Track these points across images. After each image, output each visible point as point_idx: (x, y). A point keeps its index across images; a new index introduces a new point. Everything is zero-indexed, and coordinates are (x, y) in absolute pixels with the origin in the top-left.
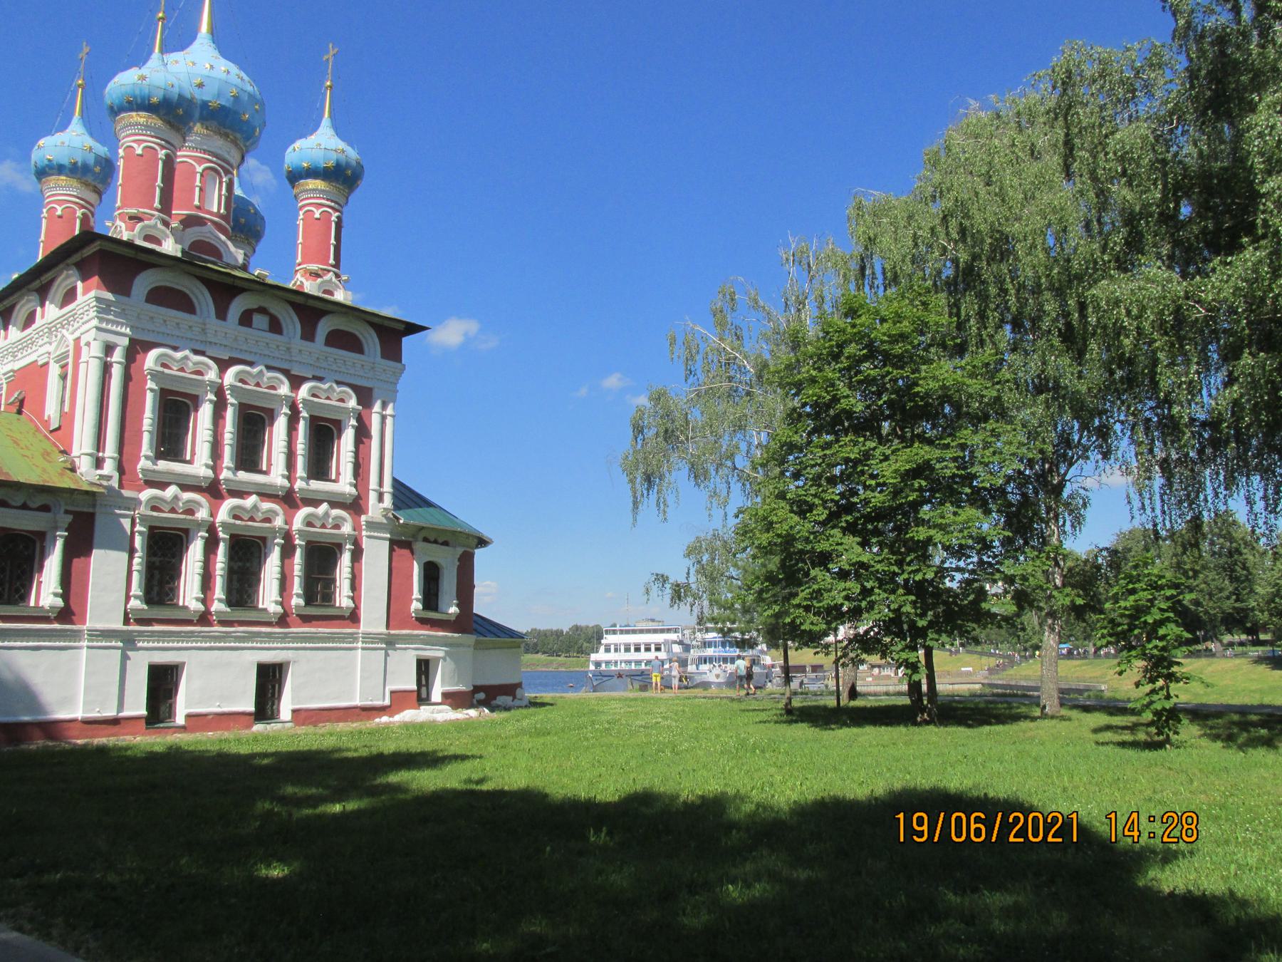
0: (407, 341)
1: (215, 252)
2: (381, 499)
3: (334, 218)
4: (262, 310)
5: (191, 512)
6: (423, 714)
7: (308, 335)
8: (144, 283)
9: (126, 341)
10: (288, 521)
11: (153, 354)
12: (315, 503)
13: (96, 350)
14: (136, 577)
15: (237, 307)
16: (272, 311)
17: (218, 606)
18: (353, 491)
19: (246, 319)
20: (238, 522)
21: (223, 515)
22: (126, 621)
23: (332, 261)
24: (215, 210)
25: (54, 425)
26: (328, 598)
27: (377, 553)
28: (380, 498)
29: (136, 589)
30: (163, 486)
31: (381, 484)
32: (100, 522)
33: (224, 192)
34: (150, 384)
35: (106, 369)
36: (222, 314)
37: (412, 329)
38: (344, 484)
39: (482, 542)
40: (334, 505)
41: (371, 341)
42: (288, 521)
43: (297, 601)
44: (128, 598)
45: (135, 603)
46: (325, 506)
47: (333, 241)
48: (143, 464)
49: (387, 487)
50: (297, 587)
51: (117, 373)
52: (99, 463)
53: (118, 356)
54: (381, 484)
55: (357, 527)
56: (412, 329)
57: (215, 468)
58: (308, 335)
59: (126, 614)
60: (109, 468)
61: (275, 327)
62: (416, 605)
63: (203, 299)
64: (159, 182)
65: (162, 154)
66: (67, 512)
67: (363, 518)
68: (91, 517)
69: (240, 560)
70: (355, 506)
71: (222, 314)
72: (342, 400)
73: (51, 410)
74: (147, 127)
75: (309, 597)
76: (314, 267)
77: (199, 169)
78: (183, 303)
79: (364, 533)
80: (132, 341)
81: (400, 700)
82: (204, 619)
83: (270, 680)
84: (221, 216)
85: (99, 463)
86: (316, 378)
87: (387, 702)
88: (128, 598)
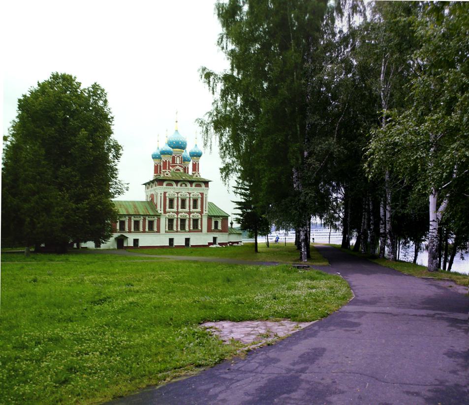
1: (179, 170)
4: (184, 183)
6: (214, 246)
7: (191, 186)
8: (165, 184)
10: (189, 216)
13: (159, 195)
15: (179, 184)
17: (179, 230)
19: (181, 186)
21: (179, 216)
27: (205, 220)
29: (167, 227)
32: (161, 219)
34: (167, 198)
36: (177, 186)
37: (211, 181)
38: (199, 210)
41: (203, 185)
42: (189, 216)
43: (192, 228)
45: (167, 230)
48: (167, 210)
49: (207, 209)
50: (191, 226)
51: (162, 198)
52: (161, 210)
53: (163, 195)
55: (202, 216)
56: (211, 181)
57: (178, 209)
58: (191, 186)
60: (162, 212)
61: (186, 186)
62: (213, 228)
63: (174, 184)
67: (203, 214)
68: (160, 218)
70: (201, 213)
71: (177, 186)
73: (155, 202)
75: (194, 228)
78: (172, 185)
81: (210, 244)
82: (177, 232)
83: (187, 240)
87: (207, 244)
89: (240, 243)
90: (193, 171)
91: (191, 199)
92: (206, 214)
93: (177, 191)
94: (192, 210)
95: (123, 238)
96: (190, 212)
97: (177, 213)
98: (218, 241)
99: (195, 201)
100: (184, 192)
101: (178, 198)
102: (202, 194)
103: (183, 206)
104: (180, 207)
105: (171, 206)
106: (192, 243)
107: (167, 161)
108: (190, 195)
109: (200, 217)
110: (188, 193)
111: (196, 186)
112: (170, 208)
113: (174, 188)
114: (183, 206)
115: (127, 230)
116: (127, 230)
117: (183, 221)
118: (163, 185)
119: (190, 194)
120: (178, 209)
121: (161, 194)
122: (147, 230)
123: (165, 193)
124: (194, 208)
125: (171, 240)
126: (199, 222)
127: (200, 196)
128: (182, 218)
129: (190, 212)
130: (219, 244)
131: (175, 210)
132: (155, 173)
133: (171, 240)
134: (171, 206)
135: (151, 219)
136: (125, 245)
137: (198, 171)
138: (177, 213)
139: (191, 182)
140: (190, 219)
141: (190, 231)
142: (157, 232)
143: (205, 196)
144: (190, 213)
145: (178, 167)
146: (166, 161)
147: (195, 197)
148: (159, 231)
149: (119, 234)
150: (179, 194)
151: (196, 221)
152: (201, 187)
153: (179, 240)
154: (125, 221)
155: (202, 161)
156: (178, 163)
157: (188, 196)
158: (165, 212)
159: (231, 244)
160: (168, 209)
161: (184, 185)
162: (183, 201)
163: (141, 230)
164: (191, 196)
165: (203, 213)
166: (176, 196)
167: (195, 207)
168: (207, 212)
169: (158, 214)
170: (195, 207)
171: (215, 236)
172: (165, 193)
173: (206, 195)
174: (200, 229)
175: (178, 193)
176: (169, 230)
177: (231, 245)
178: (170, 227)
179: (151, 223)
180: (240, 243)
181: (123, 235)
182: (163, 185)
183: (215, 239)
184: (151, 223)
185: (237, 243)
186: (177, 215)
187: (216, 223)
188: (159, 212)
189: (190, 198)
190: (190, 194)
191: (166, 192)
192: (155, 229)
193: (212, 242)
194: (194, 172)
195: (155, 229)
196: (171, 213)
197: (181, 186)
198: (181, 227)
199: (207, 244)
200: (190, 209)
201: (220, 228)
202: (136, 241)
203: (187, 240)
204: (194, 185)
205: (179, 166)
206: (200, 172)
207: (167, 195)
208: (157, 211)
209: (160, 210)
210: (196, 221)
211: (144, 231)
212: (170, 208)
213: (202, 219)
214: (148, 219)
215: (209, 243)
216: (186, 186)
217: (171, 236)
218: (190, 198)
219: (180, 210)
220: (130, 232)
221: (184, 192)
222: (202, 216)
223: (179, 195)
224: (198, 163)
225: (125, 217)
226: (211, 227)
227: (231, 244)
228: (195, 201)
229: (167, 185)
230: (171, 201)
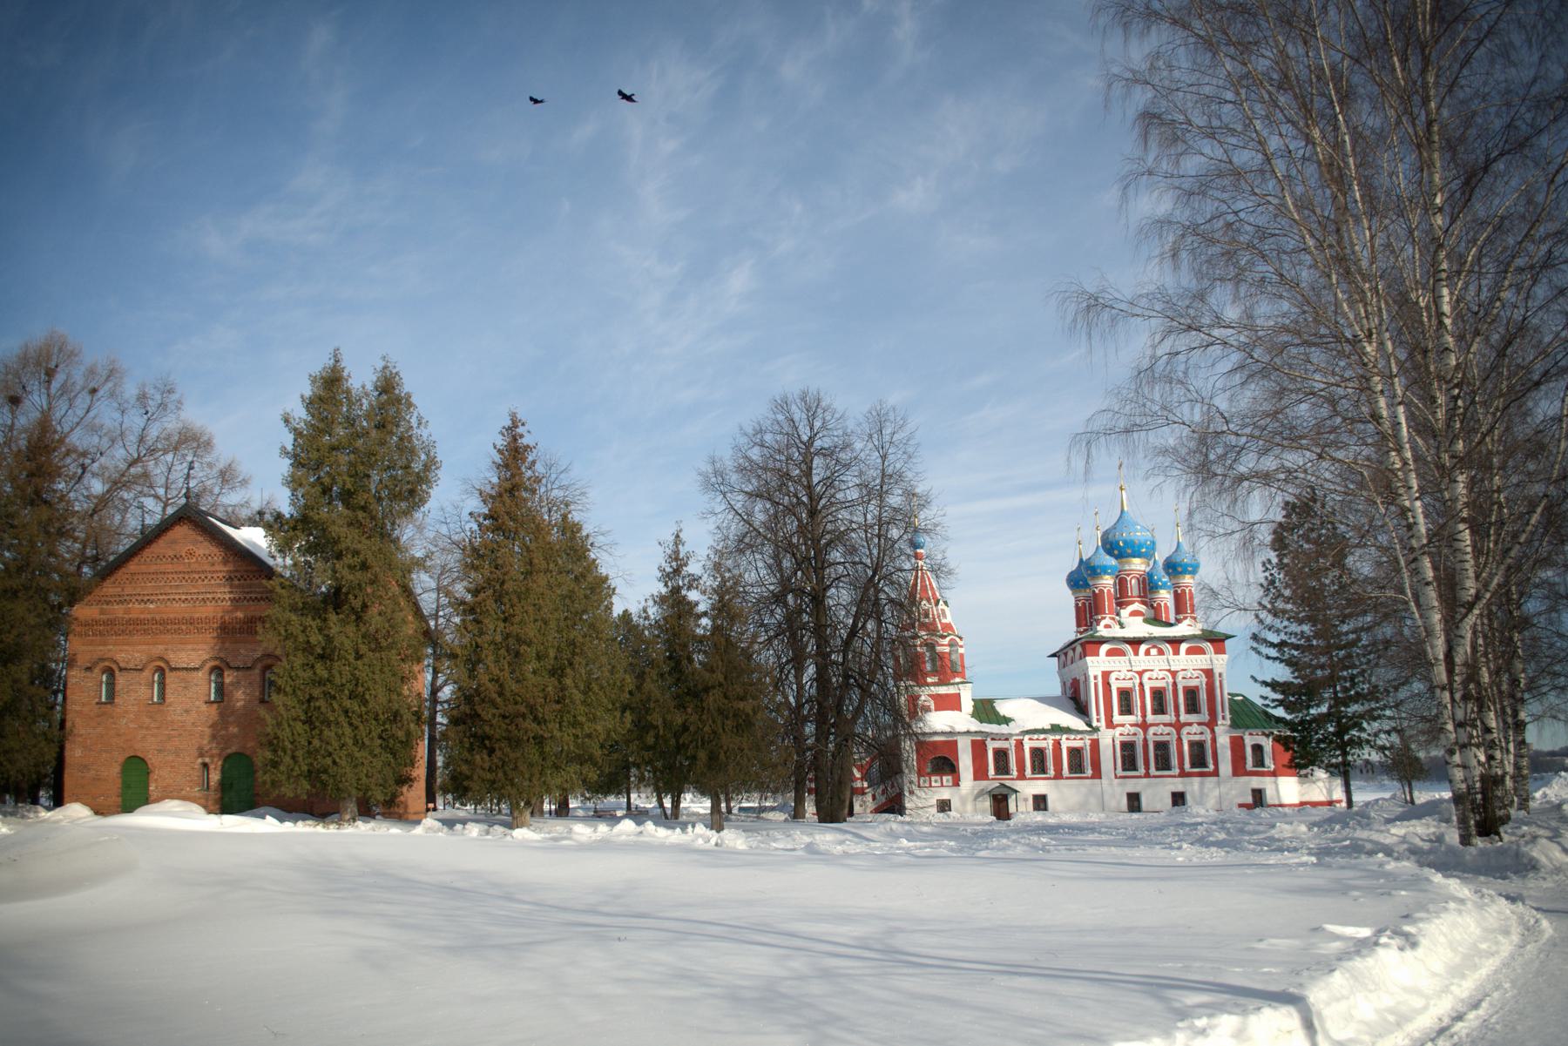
0: (1227, 642)
7: (1176, 652)
10: (1179, 733)
12: (1190, 724)
15: (1143, 648)
17: (1153, 771)
19: (1147, 653)
26: (1204, 765)
36: (1136, 653)
38: (1205, 716)
42: (1179, 733)
45: (1120, 772)
57: (1144, 715)
58: (1176, 652)
60: (1103, 724)
61: (1161, 652)
70: (1211, 724)
71: (1136, 653)
75: (1193, 765)
78: (1122, 653)
82: (1147, 775)
90: (1178, 612)
94: (1184, 718)
95: (1005, 791)
103: (1160, 709)
112: (1122, 713)
115: (1015, 773)
118: (1097, 654)
119: (1174, 674)
120: (1144, 715)
123: (1106, 675)
124: (1188, 712)
127: (1204, 680)
132: (1078, 625)
134: (1127, 709)
140: (1180, 740)
141: (1183, 774)
142: (1093, 777)
148: (1097, 774)
150: (1146, 675)
156: (1136, 592)
158: (1110, 724)
160: (1117, 718)
161: (1154, 651)
162: (1158, 695)
163: (1052, 773)
164: (1180, 675)
166: (1137, 681)
170: (1193, 707)
172: (1106, 675)
174: (1211, 767)
175: (1141, 674)
176: (1124, 770)
178: (1129, 762)
182: (1097, 654)
186: (1145, 732)
187: (1258, 749)
188: (1095, 724)
195: (1089, 772)
197: (1147, 653)
204: (1184, 647)
207: (1112, 680)
211: (1058, 776)
213: (1214, 740)
220: (1022, 776)
222: (1213, 731)
223: (1145, 680)
229: (1110, 653)
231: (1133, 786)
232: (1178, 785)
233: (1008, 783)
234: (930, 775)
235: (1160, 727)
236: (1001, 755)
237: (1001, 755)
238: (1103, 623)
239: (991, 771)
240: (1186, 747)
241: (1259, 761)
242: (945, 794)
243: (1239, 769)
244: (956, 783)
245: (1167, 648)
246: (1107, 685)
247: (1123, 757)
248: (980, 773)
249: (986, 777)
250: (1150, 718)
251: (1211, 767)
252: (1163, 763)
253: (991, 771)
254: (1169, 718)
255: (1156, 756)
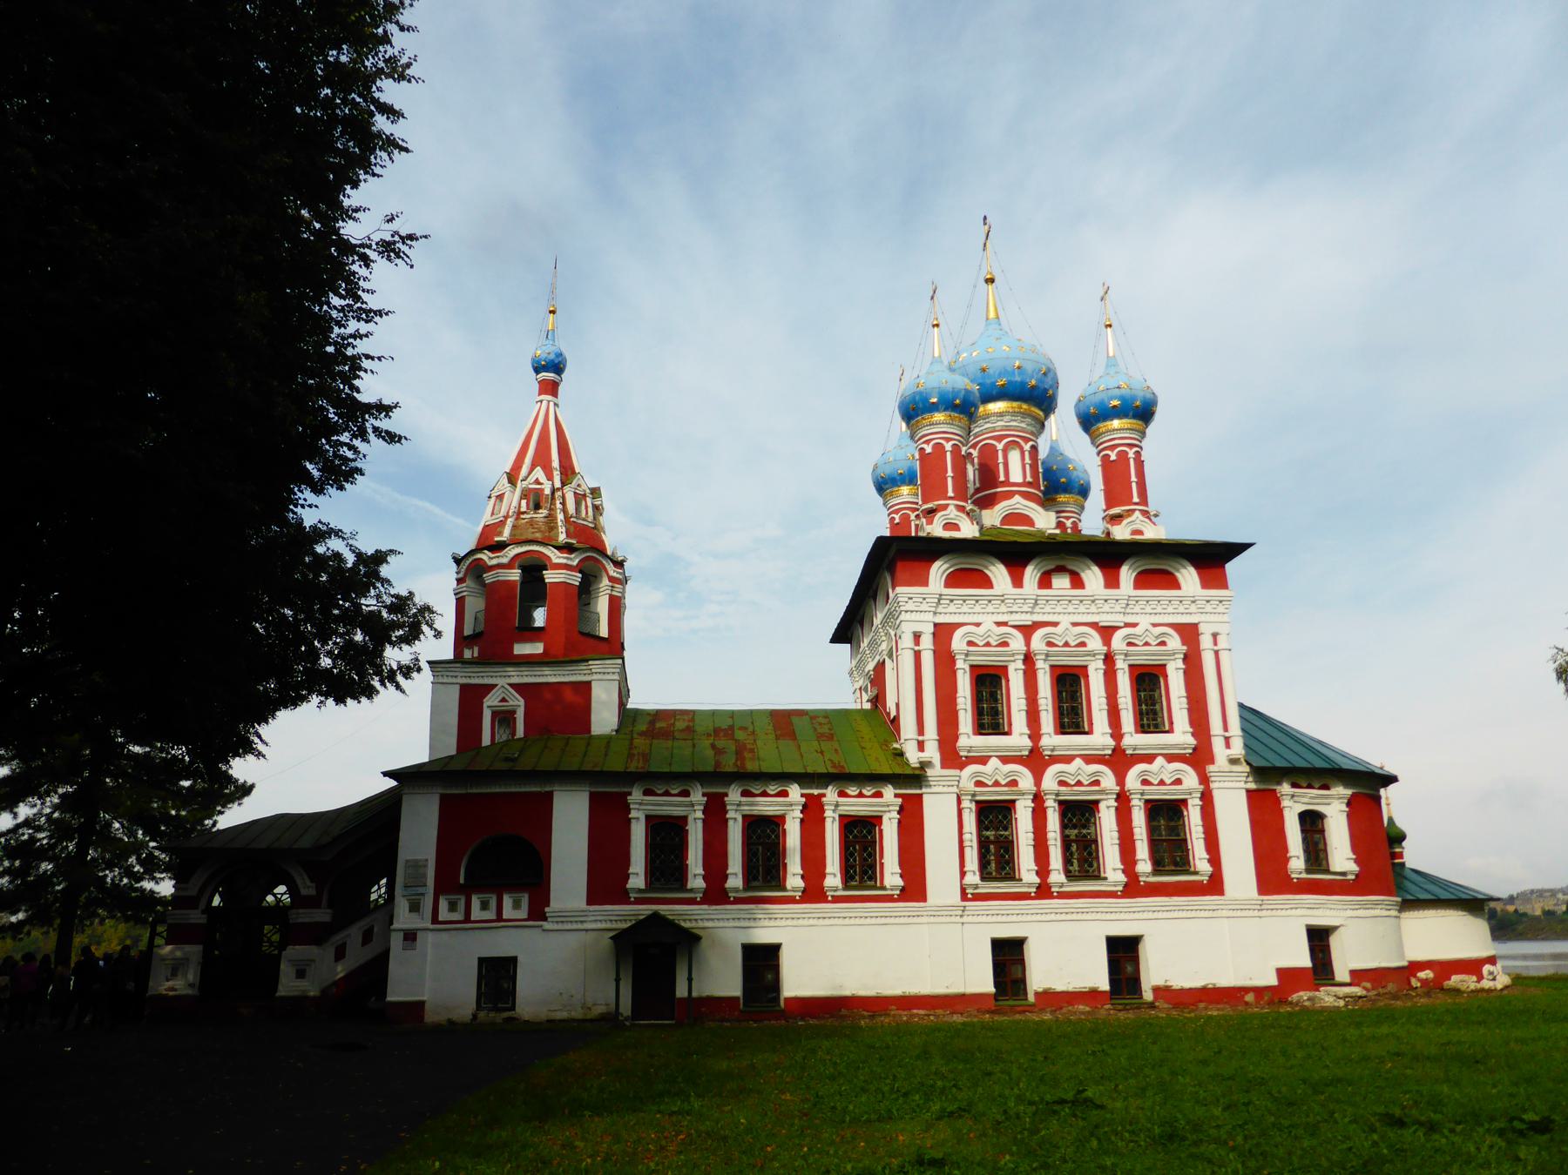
1: (1027, 520)
2: (1227, 740)
3: (1131, 454)
4: (1061, 570)
5: (1014, 783)
6: (1327, 997)
7: (1112, 582)
8: (939, 570)
9: (931, 629)
10: (1121, 781)
11: (958, 634)
12: (1150, 759)
13: (907, 642)
14: (968, 851)
15: (1031, 574)
16: (1070, 567)
17: (1057, 877)
18: (1192, 741)
19: (1045, 582)
20: (1063, 789)
21: (1049, 782)
22: (964, 896)
23: (1136, 499)
24: (1020, 480)
25: (893, 714)
28: (1227, 740)
29: (972, 863)
30: (983, 760)
31: (1226, 729)
32: (926, 798)
33: (1027, 460)
34: (960, 664)
35: (917, 655)
36: (1018, 582)
37: (1234, 550)
38: (1181, 735)
39: (1390, 779)
40: (1171, 758)
41: (1188, 576)
42: (1121, 781)
43: (1144, 866)
44: (963, 874)
45: (973, 878)
46: (1160, 761)
47: (1134, 478)
50: (1142, 851)
52: (921, 746)
53: (927, 643)
54: (1226, 729)
55: (1204, 779)
56: (1234, 550)
57: (1035, 735)
58: (1112, 582)
59: (963, 890)
60: (932, 753)
61: (1077, 583)
62: (1297, 863)
63: (998, 573)
64: (950, 473)
65: (948, 446)
66: (896, 796)
67: (1210, 768)
68: (920, 796)
69: (1075, 827)
70: (1199, 757)
71: (1018, 582)
72: (1163, 643)
74: (1014, 414)
75: (1158, 866)
76: (1116, 511)
77: (1000, 446)
79: (1212, 785)
80: (936, 625)
82: (1044, 891)
83: (1123, 951)
84: (1029, 484)
85: (921, 746)
86: (1127, 625)
87: (1272, 980)
88: (963, 874)
89: (1487, 968)
90: (1111, 501)
91: (1121, 665)
92: (1234, 761)
93: (1027, 620)
94: (1134, 740)
96: (1118, 750)
97: (1036, 760)
98: (1347, 957)
99: (1148, 680)
100: (1065, 621)
101: (1029, 659)
102: (1189, 633)
104: (1047, 720)
105: (990, 719)
106: (1160, 969)
107: (948, 446)
108: (1107, 641)
109: (1191, 780)
110: (1094, 625)
111: (1143, 581)
112: (980, 729)
113: (1002, 599)
114: (1071, 718)
115: (697, 882)
116: (697, 882)
117: (1079, 813)
118: (925, 583)
119: (1107, 632)
120: (1035, 735)
121: (917, 637)
122: (833, 880)
123: (943, 632)
125: (1008, 954)
126: (1194, 816)
127: (1175, 643)
128: (1069, 795)
129: (1118, 750)
130: (1358, 976)
131: (1018, 739)
133: (1008, 954)
135: (858, 804)
136: (681, 991)
137: (1144, 499)
138: (1036, 760)
139: (1109, 555)
140: (1123, 799)
141: (1133, 888)
143: (1206, 642)
144: (1119, 760)
145: (1018, 504)
146: (939, 448)
147: (1143, 657)
148: (914, 888)
149: (646, 910)
151: (1166, 813)
152: (1177, 586)
153: (1067, 957)
154: (684, 819)
155: (1159, 448)
157: (1095, 643)
158: (952, 758)
159: (1426, 974)
160: (968, 739)
162: (1069, 682)
163: (794, 880)
164: (1118, 642)
165: (1212, 761)
167: (1151, 717)
168: (1238, 749)
169: (908, 772)
171: (1321, 919)
173: (1215, 636)
175: (1027, 631)
176: (985, 876)
177: (1434, 987)
179: (860, 832)
180: (1487, 968)
181: (655, 916)
182: (925, 583)
183: (1319, 938)
184: (860, 832)
185: (1472, 967)
187: (1312, 822)
188: (913, 756)
189: (1109, 659)
190: (1107, 632)
191: (955, 626)
192: (892, 876)
193: (1304, 961)
194: (1116, 511)
195: (892, 876)
196: (994, 763)
197: (1045, 582)
198: (1067, 861)
199: (1272, 980)
200: (1117, 734)
201: (1342, 858)
202: (762, 962)
203: (1123, 951)
204: (1127, 574)
205: (1026, 495)
206: (1152, 509)
207: (958, 643)
208: (901, 754)
209: (918, 744)
210: (1166, 813)
211: (814, 892)
212: (980, 729)
213: (1207, 798)
214: (837, 804)
215: (1281, 972)
216: (1077, 583)
217: (1008, 921)
218: (1109, 659)
219: (1051, 740)
220: (716, 894)
221: (1065, 621)
222: (1204, 779)
224: (1138, 454)
225: (686, 794)
226: (1285, 859)
227: (1426, 974)
228: (1148, 680)
229: (953, 580)
230: (988, 681)
231: (1008, 921)
232: (1126, 919)
233: (663, 909)
234: (467, 890)
235: (1074, 773)
236: (668, 835)
237: (668, 835)
238: (939, 519)
239: (637, 880)
240: (1139, 818)
241: (1316, 852)
242: (500, 944)
243: (1272, 877)
244: (538, 912)
245: (1093, 576)
246: (945, 660)
247: (983, 845)
248: (605, 882)
249: (622, 896)
250: (1051, 740)
251: (1202, 864)
252: (1082, 857)
253: (637, 880)
254: (1100, 738)
255: (1066, 843)
